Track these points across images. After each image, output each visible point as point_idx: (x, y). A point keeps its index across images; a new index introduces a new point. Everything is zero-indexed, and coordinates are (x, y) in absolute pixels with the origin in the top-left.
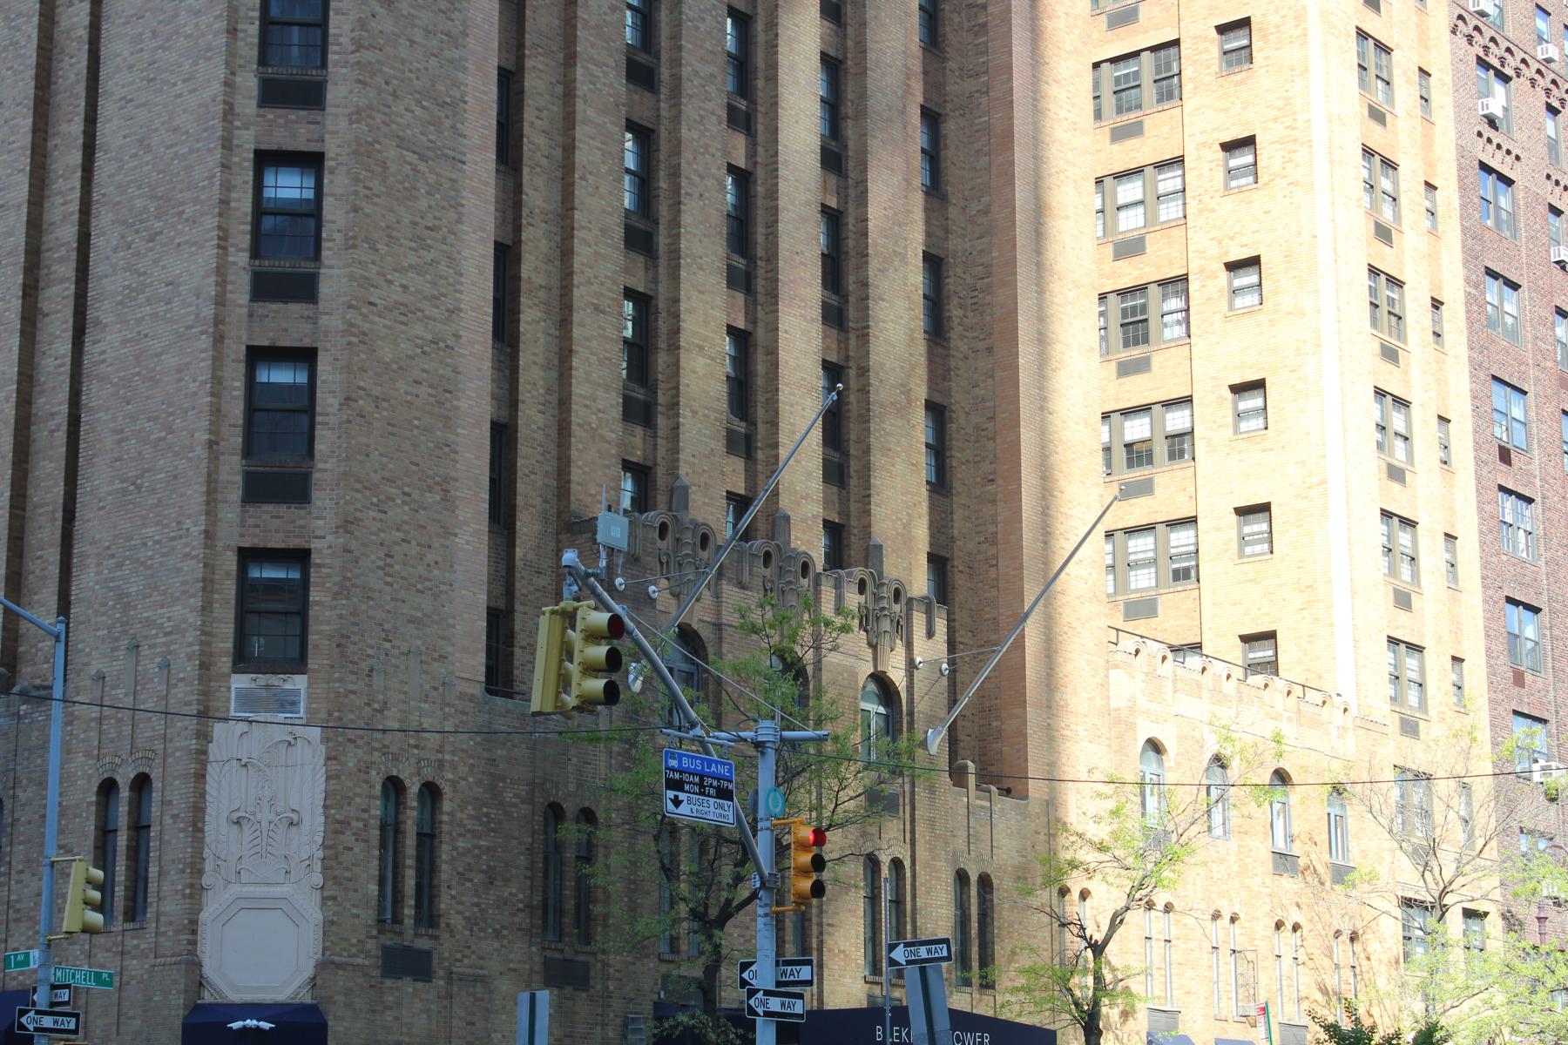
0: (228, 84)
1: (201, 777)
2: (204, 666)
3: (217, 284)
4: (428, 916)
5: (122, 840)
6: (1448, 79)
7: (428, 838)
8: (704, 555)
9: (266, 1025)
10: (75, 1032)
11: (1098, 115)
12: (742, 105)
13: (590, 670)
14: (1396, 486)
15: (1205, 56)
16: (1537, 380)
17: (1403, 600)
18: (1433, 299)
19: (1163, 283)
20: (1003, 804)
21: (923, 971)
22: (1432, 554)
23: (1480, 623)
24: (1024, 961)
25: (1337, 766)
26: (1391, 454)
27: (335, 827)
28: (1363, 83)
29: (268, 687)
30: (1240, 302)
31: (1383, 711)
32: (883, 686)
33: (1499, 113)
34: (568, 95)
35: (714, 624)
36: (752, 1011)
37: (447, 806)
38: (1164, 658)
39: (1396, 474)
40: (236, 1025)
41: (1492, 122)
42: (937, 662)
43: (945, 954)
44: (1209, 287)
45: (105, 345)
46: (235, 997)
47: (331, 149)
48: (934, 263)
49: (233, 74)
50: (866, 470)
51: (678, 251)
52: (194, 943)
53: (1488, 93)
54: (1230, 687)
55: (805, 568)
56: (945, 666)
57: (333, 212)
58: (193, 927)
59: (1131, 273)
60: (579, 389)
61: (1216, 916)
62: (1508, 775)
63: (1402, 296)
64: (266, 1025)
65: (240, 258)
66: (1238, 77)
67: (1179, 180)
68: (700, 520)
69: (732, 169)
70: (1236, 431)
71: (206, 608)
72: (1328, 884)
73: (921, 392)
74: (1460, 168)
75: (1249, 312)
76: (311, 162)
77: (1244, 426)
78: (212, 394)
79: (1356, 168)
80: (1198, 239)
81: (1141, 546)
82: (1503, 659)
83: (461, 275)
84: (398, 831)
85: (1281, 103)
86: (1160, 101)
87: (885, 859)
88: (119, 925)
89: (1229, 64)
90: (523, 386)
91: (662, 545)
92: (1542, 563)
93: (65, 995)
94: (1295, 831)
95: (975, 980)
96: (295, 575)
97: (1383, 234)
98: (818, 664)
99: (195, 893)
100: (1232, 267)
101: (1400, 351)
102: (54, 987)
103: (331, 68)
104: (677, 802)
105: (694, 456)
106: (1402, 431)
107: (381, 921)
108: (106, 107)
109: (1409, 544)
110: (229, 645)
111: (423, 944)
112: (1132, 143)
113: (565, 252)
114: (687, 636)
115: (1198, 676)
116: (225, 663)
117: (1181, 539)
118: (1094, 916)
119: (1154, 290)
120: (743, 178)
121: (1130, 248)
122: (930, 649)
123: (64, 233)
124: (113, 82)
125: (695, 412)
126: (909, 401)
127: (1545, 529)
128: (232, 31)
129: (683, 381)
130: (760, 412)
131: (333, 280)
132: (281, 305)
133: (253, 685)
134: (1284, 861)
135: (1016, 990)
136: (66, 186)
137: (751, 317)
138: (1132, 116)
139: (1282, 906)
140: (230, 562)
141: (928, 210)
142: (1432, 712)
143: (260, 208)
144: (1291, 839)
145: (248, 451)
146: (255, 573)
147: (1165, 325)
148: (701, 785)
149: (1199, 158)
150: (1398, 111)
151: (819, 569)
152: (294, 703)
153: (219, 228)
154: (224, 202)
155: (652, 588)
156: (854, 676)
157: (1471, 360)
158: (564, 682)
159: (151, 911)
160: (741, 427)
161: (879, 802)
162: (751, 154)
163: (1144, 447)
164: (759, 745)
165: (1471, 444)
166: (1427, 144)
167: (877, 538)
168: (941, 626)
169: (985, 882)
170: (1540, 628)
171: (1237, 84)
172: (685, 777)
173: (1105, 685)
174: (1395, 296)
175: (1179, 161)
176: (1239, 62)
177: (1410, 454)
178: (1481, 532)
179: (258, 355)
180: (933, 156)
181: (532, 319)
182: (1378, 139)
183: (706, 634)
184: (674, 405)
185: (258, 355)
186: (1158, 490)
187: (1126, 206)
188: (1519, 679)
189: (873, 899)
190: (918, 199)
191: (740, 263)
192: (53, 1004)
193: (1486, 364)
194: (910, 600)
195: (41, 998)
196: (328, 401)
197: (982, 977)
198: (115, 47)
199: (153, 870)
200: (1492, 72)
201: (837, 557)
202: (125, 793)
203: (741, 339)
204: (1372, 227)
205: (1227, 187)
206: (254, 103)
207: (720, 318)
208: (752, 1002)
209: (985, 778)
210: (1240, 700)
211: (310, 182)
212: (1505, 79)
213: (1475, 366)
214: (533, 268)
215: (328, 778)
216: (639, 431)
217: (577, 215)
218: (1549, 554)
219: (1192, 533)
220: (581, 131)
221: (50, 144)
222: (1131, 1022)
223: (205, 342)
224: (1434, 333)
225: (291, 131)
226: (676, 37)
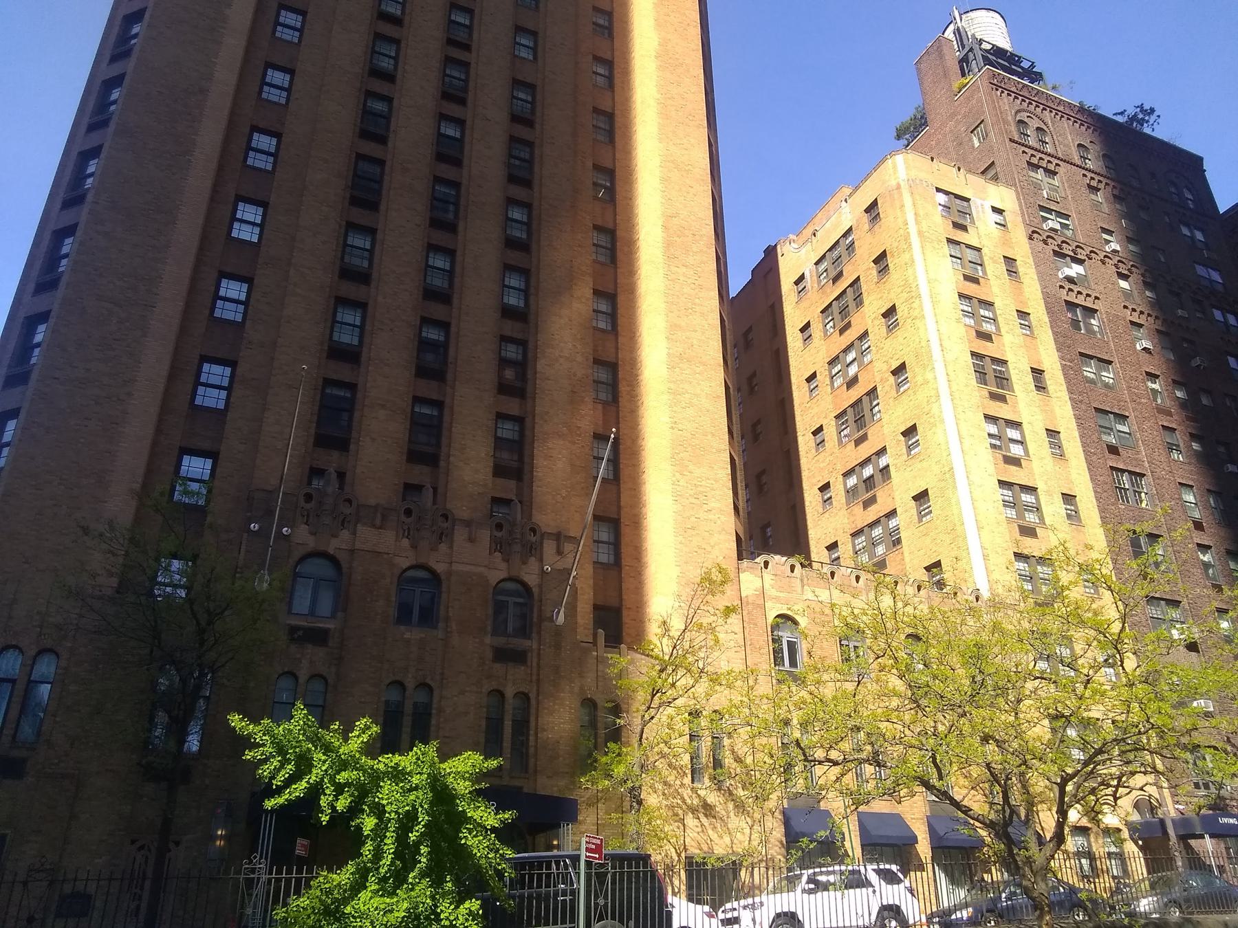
19: (868, 394)
35: (350, 550)
44: (886, 386)
63: (1007, 368)
83: (141, 363)
87: (509, 692)
91: (308, 506)
101: (1007, 396)
105: (370, 462)
109: (1034, 501)
112: (848, 332)
127: (1156, 490)
130: (444, 441)
165: (1080, 444)
171: (885, 283)
174: (1004, 369)
178: (1095, 492)
186: (879, 499)
194: (543, 535)
200: (1068, 258)
204: (974, 333)
213: (1075, 404)
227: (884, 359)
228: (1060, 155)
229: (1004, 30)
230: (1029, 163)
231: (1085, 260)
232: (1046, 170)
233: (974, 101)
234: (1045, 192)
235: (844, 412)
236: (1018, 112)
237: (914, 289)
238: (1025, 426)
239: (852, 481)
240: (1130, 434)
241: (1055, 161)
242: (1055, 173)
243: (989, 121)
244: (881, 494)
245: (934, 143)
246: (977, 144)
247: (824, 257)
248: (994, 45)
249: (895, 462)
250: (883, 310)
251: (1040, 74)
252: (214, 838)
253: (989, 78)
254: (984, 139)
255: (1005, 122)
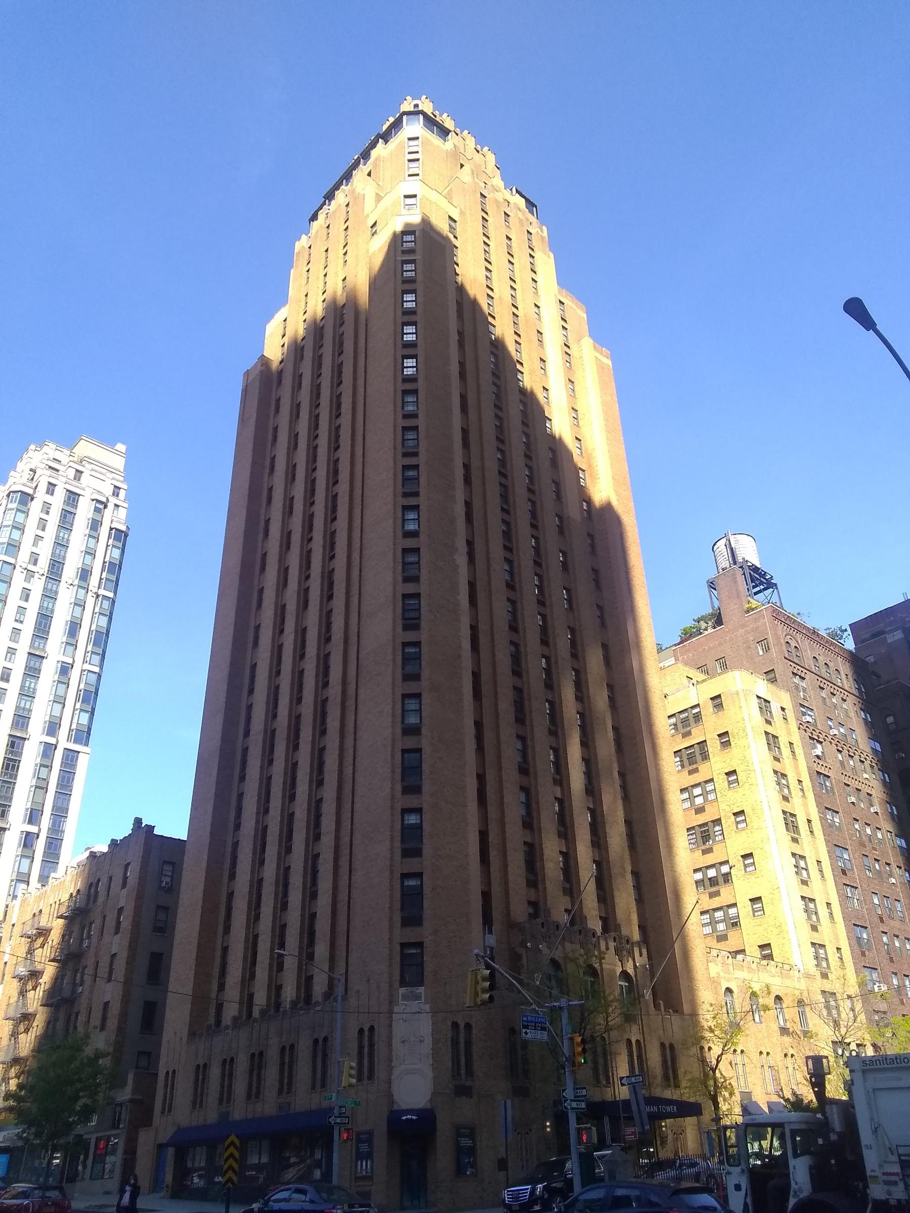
0: (392, 789)
1: (390, 1026)
2: (391, 986)
3: (391, 854)
4: (470, 1073)
5: (366, 1050)
6: (800, 745)
7: (468, 1044)
8: (557, 933)
9: (414, 1118)
10: (348, 1123)
11: (683, 766)
12: (558, 777)
13: (484, 991)
14: (805, 887)
15: (715, 744)
16: (851, 845)
17: (814, 928)
18: (808, 820)
19: (713, 821)
20: (675, 1018)
21: (634, 1087)
22: (823, 911)
23: (845, 934)
24: (689, 1077)
25: (797, 993)
26: (801, 875)
27: (436, 1041)
28: (770, 749)
29: (412, 992)
30: (739, 826)
31: (813, 970)
32: (625, 975)
33: (820, 754)
34: (500, 780)
36: (566, 1108)
37: (474, 1031)
38: (728, 957)
39: (804, 882)
40: (404, 1118)
41: (818, 757)
42: (644, 966)
43: (641, 1080)
44: (728, 822)
45: (358, 876)
46: (404, 1107)
47: (425, 807)
48: (628, 823)
49: (393, 785)
50: (613, 897)
51: (540, 827)
52: (390, 1087)
53: (815, 748)
54: (754, 966)
55: (594, 934)
56: (647, 966)
57: (426, 827)
58: (389, 1082)
59: (702, 819)
60: (511, 877)
61: (768, 1054)
62: (866, 994)
63: (796, 819)
64: (414, 1118)
65: (398, 844)
66: (727, 751)
67: (713, 786)
68: (556, 920)
69: (556, 798)
70: (746, 872)
71: (390, 965)
72: (802, 1038)
73: (629, 868)
74: (809, 774)
75: (743, 829)
76: (419, 811)
77: (748, 869)
78: (390, 891)
79: (773, 778)
80: (723, 806)
81: (719, 915)
82: (856, 947)
84: (458, 1042)
85: (743, 758)
86: (703, 760)
88: (365, 1081)
89: (724, 746)
90: (492, 877)
91: (543, 930)
92: (865, 910)
93: (343, 1110)
94: (787, 1018)
95: (672, 1084)
96: (419, 951)
97: (786, 799)
98: (602, 969)
99: (390, 1069)
100: (735, 814)
102: (340, 1107)
103: (423, 780)
104: (526, 1033)
106: (805, 867)
107: (453, 1076)
108: (357, 799)
110: (398, 978)
111: (468, 1083)
112: (696, 775)
113: (503, 832)
114: (554, 963)
115: (742, 963)
116: (397, 984)
117: (732, 911)
118: (712, 1056)
119: (710, 824)
120: (560, 801)
121: (700, 810)
122: (641, 960)
123: (346, 839)
124: (359, 791)
125: (551, 882)
126: (625, 872)
128: (393, 772)
129: (546, 871)
131: (427, 850)
132: (410, 859)
133: (406, 991)
134: (784, 1031)
135: (686, 1087)
136: (346, 824)
137: (567, 847)
138: (694, 766)
139: (786, 1048)
140: (398, 948)
141: (624, 805)
142: (832, 969)
143: (404, 828)
144: (785, 1021)
145: (402, 909)
146: (406, 951)
147: (716, 836)
148: (535, 1026)
149: (718, 778)
150: (784, 756)
151: (599, 934)
152: (420, 997)
153: (391, 835)
154: (392, 827)
155: (540, 946)
156: (614, 971)
157: (825, 839)
158: (476, 994)
159: (376, 1076)
160: (568, 886)
161: (629, 1018)
162: (562, 793)
163: (715, 879)
164: (561, 1008)
166: (796, 767)
167: (619, 921)
168: (644, 951)
169: (672, 1047)
170: (868, 935)
172: (529, 1024)
173: (707, 969)
174: (794, 820)
175: (712, 780)
176: (727, 746)
177: (808, 874)
178: (839, 901)
179: (404, 876)
180: (624, 787)
181: (493, 855)
182: (778, 766)
183: (561, 961)
184: (544, 880)
185: (404, 876)
187: (697, 796)
188: (863, 954)
189: (631, 1055)
190: (620, 803)
191: (562, 829)
192: (340, 1114)
193: (831, 840)
195: (336, 1112)
196: (427, 889)
197: (675, 1083)
198: (360, 779)
199: (376, 1061)
200: (815, 741)
201: (606, 929)
202: (366, 1033)
203: (565, 855)
205: (729, 788)
206: (400, 793)
207: (557, 849)
208: (566, 1104)
209: (667, 1007)
210: (759, 970)
211: (419, 817)
212: (821, 743)
213: (827, 841)
214: (493, 838)
215: (433, 1023)
216: (533, 890)
217: (506, 819)
218: (867, 907)
219: (736, 908)
220: (505, 791)
221: (342, 811)
222: (733, 1097)
223: (387, 873)
224: (810, 831)
225: (412, 801)
226: (534, 758)
227: (727, 803)
228: (806, 667)
229: (755, 548)
230: (793, 673)
231: (822, 742)
232: (800, 677)
233: (760, 623)
234: (801, 693)
235: (693, 828)
236: (786, 636)
237: (750, 765)
238: (807, 858)
239: (699, 876)
240: (849, 860)
241: (805, 671)
242: (804, 679)
243: (771, 640)
244: (724, 890)
245: (728, 638)
246: (761, 653)
247: (673, 715)
248: (753, 565)
249: (736, 873)
250: (727, 771)
251: (776, 585)
252: (546, 1127)
253: (772, 613)
254: (766, 651)
255: (781, 644)
